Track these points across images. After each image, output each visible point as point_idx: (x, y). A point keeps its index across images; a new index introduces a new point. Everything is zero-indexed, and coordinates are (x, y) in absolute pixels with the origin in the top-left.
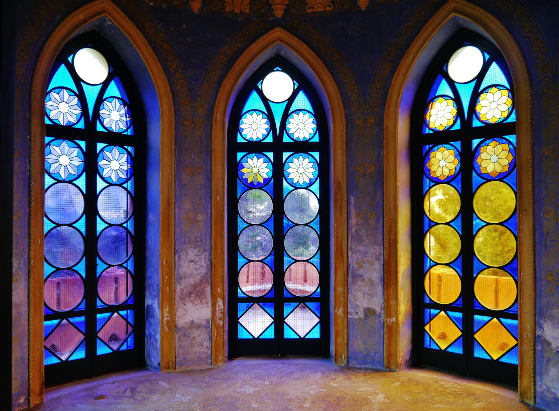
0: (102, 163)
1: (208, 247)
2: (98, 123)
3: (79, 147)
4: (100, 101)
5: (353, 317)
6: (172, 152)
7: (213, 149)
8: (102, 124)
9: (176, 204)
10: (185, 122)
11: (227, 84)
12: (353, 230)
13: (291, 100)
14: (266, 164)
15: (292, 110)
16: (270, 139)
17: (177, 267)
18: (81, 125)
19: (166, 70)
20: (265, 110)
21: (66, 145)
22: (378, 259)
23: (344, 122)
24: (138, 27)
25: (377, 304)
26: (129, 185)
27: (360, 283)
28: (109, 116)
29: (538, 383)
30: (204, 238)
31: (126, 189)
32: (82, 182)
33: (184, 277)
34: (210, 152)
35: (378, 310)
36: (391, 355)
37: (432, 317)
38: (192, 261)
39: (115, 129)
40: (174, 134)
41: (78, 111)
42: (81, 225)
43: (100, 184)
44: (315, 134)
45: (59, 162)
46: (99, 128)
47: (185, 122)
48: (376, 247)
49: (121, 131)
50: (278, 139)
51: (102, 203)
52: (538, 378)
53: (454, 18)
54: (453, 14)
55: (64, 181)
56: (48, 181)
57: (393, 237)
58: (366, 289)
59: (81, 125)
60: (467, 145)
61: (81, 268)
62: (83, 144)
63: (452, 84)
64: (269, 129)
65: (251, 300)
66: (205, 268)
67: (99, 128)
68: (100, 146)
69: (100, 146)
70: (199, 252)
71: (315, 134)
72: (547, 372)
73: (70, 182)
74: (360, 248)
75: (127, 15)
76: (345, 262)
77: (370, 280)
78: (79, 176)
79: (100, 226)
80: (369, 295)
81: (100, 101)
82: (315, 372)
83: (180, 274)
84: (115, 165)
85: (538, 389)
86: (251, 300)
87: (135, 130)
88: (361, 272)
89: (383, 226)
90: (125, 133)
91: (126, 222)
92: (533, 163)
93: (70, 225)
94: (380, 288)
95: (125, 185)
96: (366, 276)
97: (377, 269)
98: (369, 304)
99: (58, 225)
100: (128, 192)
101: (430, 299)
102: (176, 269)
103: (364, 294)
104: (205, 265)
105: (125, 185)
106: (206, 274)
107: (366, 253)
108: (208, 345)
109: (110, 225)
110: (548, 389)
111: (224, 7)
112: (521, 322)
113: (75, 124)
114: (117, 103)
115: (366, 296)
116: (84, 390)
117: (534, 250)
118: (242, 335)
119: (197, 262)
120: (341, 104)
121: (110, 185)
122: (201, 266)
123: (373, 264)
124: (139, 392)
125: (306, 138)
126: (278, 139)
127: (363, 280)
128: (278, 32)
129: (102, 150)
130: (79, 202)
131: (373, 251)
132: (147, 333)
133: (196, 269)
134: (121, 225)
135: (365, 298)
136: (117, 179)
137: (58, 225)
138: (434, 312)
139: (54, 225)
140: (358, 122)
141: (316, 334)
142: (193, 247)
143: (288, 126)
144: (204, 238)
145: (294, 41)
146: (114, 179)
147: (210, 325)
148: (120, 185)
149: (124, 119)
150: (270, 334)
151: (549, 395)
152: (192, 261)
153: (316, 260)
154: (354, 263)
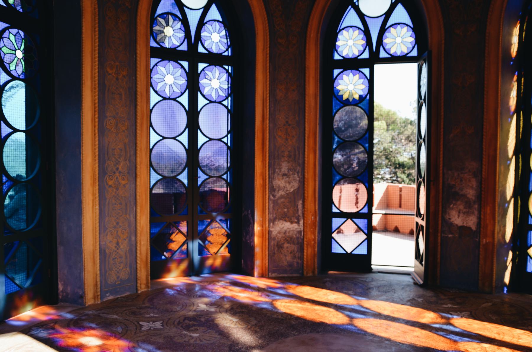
0: (203, 81)
1: (301, 161)
2: (200, 44)
3: (182, 67)
4: (201, 24)
5: (446, 236)
6: (266, 70)
7: (306, 66)
8: (203, 46)
9: (271, 119)
15: (389, 23)
17: (270, 180)
18: (184, 47)
20: (361, 26)
21: (171, 65)
28: (209, 38)
30: (297, 153)
32: (184, 100)
33: (277, 190)
35: (474, 228)
38: (284, 175)
39: (214, 50)
40: (268, 52)
41: (182, 35)
42: (184, 138)
43: (201, 101)
44: (413, 48)
45: (164, 81)
46: (201, 50)
49: (220, 52)
55: (169, 99)
59: (184, 47)
62: (185, 64)
64: (365, 45)
66: (298, 182)
67: (201, 50)
68: (201, 66)
69: (201, 66)
70: (292, 166)
71: (413, 48)
73: (175, 99)
78: (182, 94)
80: (464, 213)
81: (201, 24)
83: (273, 187)
84: (215, 84)
97: (474, 186)
98: (463, 223)
102: (270, 182)
103: (459, 212)
104: (298, 179)
106: (299, 188)
108: (300, 256)
109: (211, 139)
113: (179, 46)
115: (461, 215)
119: (290, 176)
121: (211, 102)
122: (294, 180)
123: (470, 181)
125: (404, 53)
129: (203, 70)
130: (182, 120)
132: (244, 240)
133: (289, 183)
134: (220, 140)
135: (461, 216)
136: (216, 98)
139: (161, 138)
142: (286, 161)
143: (385, 41)
144: (297, 153)
146: (214, 97)
147: (302, 237)
148: (220, 103)
152: (284, 175)
154: (449, 180)
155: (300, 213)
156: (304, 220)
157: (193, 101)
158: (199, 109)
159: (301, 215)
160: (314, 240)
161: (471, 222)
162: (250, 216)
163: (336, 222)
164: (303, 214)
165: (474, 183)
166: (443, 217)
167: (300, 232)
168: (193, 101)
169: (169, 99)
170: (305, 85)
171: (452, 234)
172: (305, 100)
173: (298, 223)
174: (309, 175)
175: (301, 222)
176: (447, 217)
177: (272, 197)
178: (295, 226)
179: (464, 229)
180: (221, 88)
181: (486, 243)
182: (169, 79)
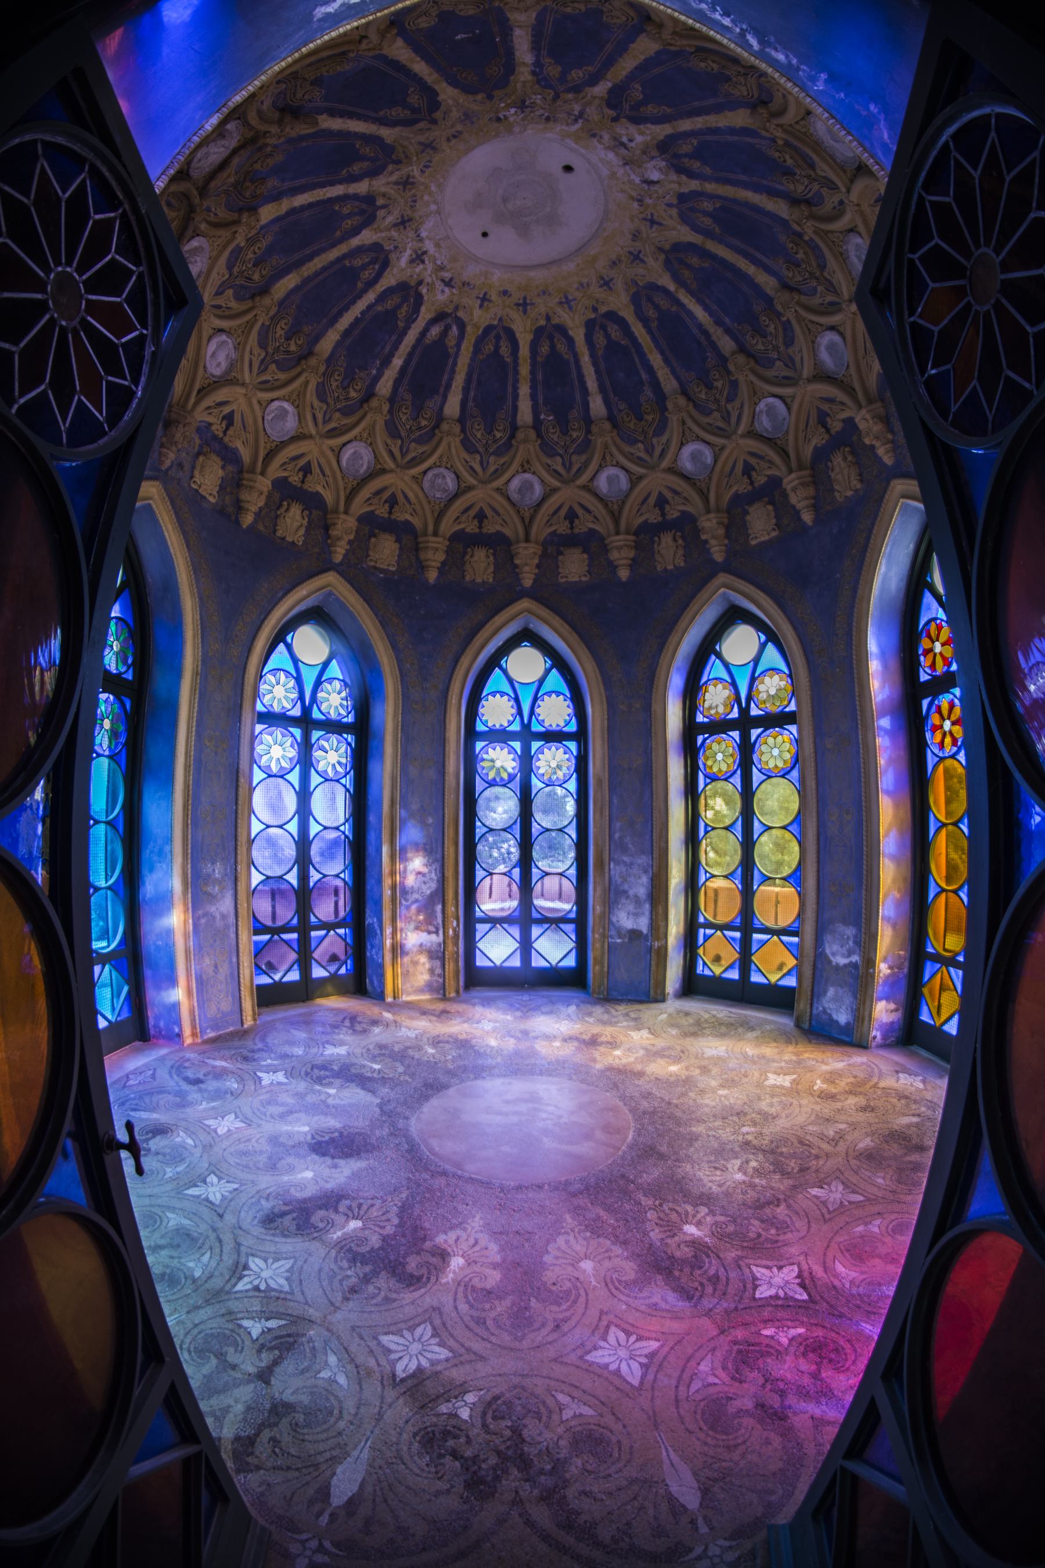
0: (317, 754)
1: (439, 856)
10: (415, 706)
11: (465, 661)
12: (617, 836)
13: (541, 682)
14: (512, 756)
16: (516, 727)
19: (394, 646)
22: (646, 872)
23: (605, 706)
24: (365, 600)
25: (643, 924)
26: (347, 781)
27: (623, 901)
29: (815, 1005)
31: (345, 786)
32: (294, 777)
34: (443, 742)
35: (645, 930)
36: (662, 983)
37: (707, 938)
39: (333, 715)
41: (294, 695)
42: (293, 827)
43: (315, 779)
47: (415, 706)
48: (644, 857)
50: (526, 727)
51: (318, 803)
52: (815, 1000)
53: (724, 594)
54: (722, 590)
55: (275, 776)
56: (258, 775)
57: (663, 844)
58: (631, 908)
60: (745, 736)
61: (293, 878)
63: (726, 665)
65: (493, 921)
72: (825, 992)
73: (282, 777)
74: (625, 859)
75: (354, 587)
76: (607, 875)
77: (636, 896)
79: (314, 829)
80: (634, 914)
82: (568, 1006)
84: (333, 757)
85: (815, 1011)
86: (493, 921)
87: (356, 716)
88: (626, 887)
89: (652, 832)
90: (345, 720)
91: (344, 824)
92: (816, 756)
93: (281, 827)
94: (647, 906)
95: (343, 781)
96: (631, 893)
99: (268, 826)
100: (347, 790)
101: (705, 918)
105: (343, 781)
106: (437, 890)
107: (632, 864)
109: (325, 828)
110: (824, 1011)
111: (464, 577)
112: (802, 940)
114: (337, 685)
115: (631, 916)
116: (300, 1015)
117: (818, 858)
118: (480, 962)
120: (601, 685)
124: (360, 1023)
126: (526, 727)
127: (628, 897)
128: (525, 603)
130: (291, 802)
131: (640, 861)
133: (425, 883)
134: (337, 828)
137: (268, 826)
138: (709, 932)
140: (622, 707)
141: (571, 962)
145: (545, 612)
148: (338, 781)
149: (345, 703)
150: (516, 962)
151: (824, 1017)
153: (573, 872)
155: (440, 920)
156: (444, 928)
157: (305, 779)
158: (312, 789)
159: (440, 922)
160: (457, 953)
161: (643, 924)
162: (376, 926)
163: (481, 928)
164: (443, 921)
165: (645, 880)
166: (609, 919)
167: (440, 944)
168: (305, 779)
169: (275, 776)
170: (444, 761)
171: (620, 938)
172: (444, 780)
173: (437, 933)
174: (449, 873)
175: (441, 932)
176: (614, 919)
177: (404, 902)
178: (433, 937)
179: (634, 934)
180: (339, 763)
181: (659, 948)
182: (277, 752)
